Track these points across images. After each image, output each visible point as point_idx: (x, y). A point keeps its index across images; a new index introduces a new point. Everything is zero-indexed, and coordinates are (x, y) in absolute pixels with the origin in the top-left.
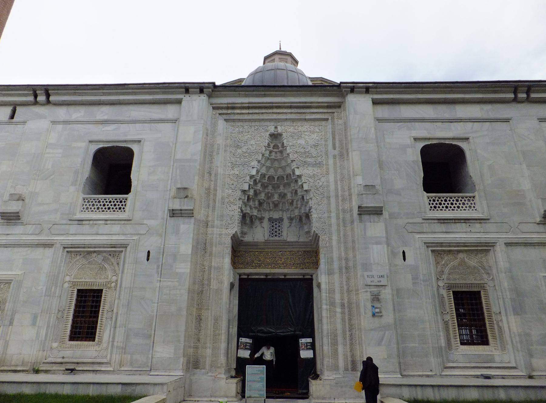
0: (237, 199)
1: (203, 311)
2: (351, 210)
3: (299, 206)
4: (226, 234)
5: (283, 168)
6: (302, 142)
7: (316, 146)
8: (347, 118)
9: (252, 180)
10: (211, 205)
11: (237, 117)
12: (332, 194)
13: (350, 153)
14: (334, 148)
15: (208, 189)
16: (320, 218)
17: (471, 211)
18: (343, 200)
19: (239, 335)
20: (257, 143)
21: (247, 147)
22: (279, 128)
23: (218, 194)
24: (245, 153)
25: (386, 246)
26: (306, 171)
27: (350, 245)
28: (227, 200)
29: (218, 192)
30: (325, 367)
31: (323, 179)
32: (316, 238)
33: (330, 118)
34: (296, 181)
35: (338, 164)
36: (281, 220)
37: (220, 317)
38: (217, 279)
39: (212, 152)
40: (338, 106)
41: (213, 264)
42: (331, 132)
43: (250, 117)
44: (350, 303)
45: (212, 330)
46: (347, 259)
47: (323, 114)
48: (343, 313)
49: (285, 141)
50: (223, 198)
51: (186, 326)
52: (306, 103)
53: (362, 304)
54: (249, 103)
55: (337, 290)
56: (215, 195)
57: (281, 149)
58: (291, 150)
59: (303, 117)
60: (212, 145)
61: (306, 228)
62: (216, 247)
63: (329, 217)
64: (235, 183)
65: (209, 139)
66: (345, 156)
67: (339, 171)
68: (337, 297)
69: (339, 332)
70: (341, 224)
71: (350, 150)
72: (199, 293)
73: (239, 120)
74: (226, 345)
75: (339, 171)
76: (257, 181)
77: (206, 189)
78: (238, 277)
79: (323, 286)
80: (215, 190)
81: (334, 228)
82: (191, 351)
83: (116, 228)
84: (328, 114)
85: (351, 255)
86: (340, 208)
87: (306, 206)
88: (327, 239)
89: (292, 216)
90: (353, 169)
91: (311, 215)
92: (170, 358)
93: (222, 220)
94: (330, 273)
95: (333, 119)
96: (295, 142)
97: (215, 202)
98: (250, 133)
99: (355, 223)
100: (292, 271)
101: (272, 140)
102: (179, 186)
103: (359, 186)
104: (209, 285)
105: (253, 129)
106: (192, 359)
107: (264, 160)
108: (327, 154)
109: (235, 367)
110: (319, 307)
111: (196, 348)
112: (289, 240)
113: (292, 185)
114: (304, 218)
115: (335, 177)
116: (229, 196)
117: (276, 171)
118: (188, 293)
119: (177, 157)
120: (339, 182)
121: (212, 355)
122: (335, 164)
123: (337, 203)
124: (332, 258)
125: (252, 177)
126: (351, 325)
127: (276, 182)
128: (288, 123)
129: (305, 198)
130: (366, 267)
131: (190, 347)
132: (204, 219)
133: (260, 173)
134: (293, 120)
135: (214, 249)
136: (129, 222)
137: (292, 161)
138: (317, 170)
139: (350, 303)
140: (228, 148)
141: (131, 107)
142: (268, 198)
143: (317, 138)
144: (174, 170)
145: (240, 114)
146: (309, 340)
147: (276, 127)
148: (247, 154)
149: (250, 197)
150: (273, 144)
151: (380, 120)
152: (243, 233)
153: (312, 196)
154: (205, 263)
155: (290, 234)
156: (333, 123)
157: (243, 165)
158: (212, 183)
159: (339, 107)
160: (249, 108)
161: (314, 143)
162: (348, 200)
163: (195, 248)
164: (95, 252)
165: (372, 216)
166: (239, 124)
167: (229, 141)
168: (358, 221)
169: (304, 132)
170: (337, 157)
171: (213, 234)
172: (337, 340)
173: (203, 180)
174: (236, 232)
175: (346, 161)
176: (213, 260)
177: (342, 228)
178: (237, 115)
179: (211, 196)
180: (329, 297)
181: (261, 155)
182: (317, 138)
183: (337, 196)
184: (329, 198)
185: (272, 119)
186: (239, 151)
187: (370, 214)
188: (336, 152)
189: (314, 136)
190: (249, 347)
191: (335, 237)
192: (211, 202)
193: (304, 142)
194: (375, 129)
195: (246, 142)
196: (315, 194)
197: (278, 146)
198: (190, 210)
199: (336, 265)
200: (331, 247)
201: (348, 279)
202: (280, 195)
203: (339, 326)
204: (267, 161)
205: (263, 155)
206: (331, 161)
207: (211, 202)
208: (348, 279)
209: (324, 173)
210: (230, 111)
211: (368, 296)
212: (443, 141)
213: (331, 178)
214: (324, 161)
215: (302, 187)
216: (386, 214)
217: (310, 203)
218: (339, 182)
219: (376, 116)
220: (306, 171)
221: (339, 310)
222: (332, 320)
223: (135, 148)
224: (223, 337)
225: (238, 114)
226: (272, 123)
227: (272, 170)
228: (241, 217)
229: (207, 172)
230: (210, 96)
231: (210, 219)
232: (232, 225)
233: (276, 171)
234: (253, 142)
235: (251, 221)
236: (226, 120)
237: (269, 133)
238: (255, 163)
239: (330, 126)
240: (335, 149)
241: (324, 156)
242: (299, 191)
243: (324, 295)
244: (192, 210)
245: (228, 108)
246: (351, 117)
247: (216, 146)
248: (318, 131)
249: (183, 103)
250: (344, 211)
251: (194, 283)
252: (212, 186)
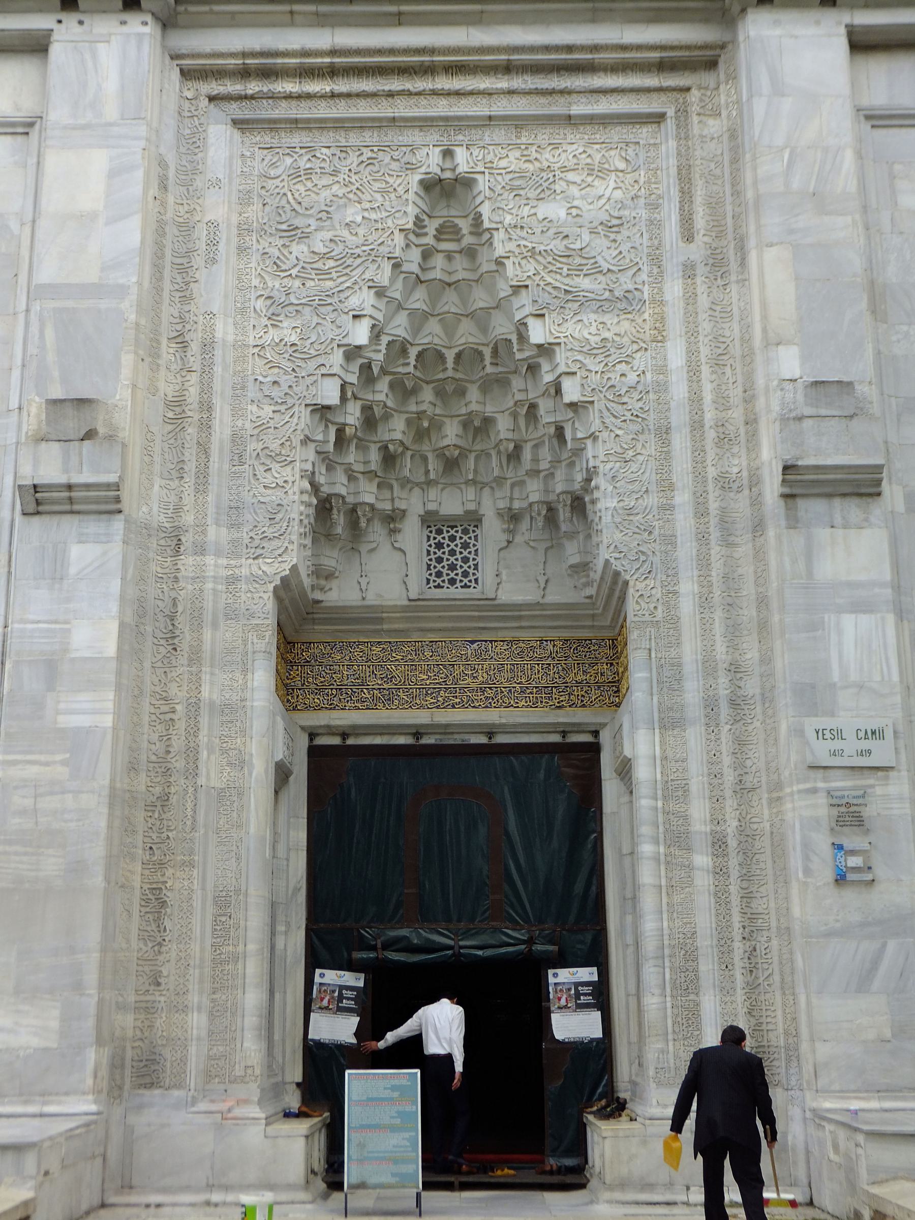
0: (296, 441)
1: (169, 872)
2: (755, 481)
3: (544, 465)
4: (255, 579)
5: (481, 319)
6: (555, 210)
7: (611, 227)
8: (740, 114)
9: (355, 367)
10: (191, 467)
11: (283, 110)
12: (679, 417)
13: (753, 257)
14: (689, 238)
15: (177, 403)
16: (630, 512)
18: (724, 440)
19: (314, 960)
20: (373, 216)
21: (328, 235)
22: (461, 156)
23: (216, 423)
24: (324, 256)
25: (891, 619)
26: (571, 328)
27: (749, 613)
28: (253, 446)
29: (217, 413)
30: (651, 1072)
31: (640, 361)
32: (615, 589)
33: (671, 112)
34: (533, 369)
35: (703, 301)
36: (472, 520)
37: (238, 891)
38: (224, 751)
39: (189, 254)
40: (707, 60)
41: (205, 693)
42: (673, 171)
43: (340, 110)
44: (747, 835)
45: (208, 942)
46: (735, 669)
47: (643, 97)
48: (720, 872)
49: (485, 210)
50: (237, 438)
51: (105, 928)
52: (570, 48)
53: (795, 839)
54: (333, 52)
55: (697, 782)
56: (206, 426)
57: (468, 240)
58: (511, 246)
59: (558, 107)
60: (186, 228)
61: (572, 553)
62: (215, 625)
63: (667, 508)
64: (285, 380)
65: (171, 199)
66: (734, 266)
67: (706, 326)
68: (699, 812)
69: (706, 942)
70: (715, 535)
71: (752, 243)
72: (153, 805)
73: (295, 124)
74: (265, 996)
75: (706, 326)
76: (376, 370)
77: (168, 405)
78: (303, 742)
79: (642, 772)
80: (207, 407)
81: (686, 550)
82: (127, 1021)
84: (663, 97)
85: (752, 655)
86: (712, 472)
87: (572, 465)
88: (658, 593)
89: (517, 505)
90: (765, 317)
91: (593, 502)
92: (46, 1050)
93: (235, 526)
94: (670, 721)
95: (683, 113)
96: (526, 211)
97: (206, 453)
98: (340, 178)
99: (771, 533)
100: (521, 719)
101: (433, 208)
102: (57, 393)
103: (789, 386)
104: (192, 772)
105: (353, 159)
106: (129, 1054)
107: (399, 285)
108: (656, 260)
109: (299, 1078)
110: (626, 850)
111: (147, 1009)
112: (507, 595)
113: (517, 383)
114: (563, 514)
115: (692, 353)
116: (262, 428)
117: (449, 330)
118: (111, 806)
119: (46, 274)
120: (705, 370)
121: (211, 1033)
122: (690, 298)
123: (699, 451)
124: (678, 665)
125: (352, 353)
126: (751, 920)
127: (450, 373)
128: (499, 135)
129: (568, 435)
130: (813, 696)
131: (121, 1007)
132: (160, 518)
133: (385, 339)
134: (518, 123)
135: (207, 635)
137: (517, 289)
138: (617, 326)
139: (747, 835)
140: (251, 240)
142: (421, 435)
143: (618, 194)
144: (34, 329)
145: (299, 97)
146: (588, 974)
147: (448, 153)
148: (331, 263)
149: (349, 431)
150: (436, 223)
151: (877, 119)
152: (323, 575)
153: (596, 425)
154: (173, 689)
155: (508, 575)
156: (683, 135)
157: (319, 304)
158: (194, 378)
159: (712, 64)
160: (333, 72)
161: (604, 217)
162: (742, 438)
163: (131, 635)
165: (837, 502)
166: (297, 139)
167: (254, 212)
168: (783, 523)
169: (564, 169)
170: (701, 270)
171: (199, 578)
172: (696, 971)
173: (155, 368)
174: (294, 568)
175: (734, 288)
176: (206, 677)
177: (716, 550)
178: (284, 104)
179: (190, 430)
180: (666, 813)
181: (387, 267)
182: (618, 194)
183: (697, 426)
184: (664, 433)
185: (432, 119)
186: (299, 250)
187: (830, 496)
188: (696, 252)
189: (606, 187)
190: (351, 1004)
191: (688, 587)
192: (191, 454)
193: (562, 213)
194: (859, 155)
195: (325, 215)
196: (609, 420)
197: (456, 230)
198: (108, 486)
199: (692, 693)
200: (674, 622)
201: (741, 743)
202: (465, 425)
203: (704, 921)
204: (412, 291)
205: (396, 266)
206: (674, 289)
207: (191, 454)
208: (741, 743)
209: (647, 337)
210: (253, 87)
211: (820, 808)
213: (676, 355)
214: (646, 289)
215: (558, 391)
216: (893, 495)
217: (590, 452)
218: (705, 370)
219: (865, 102)
220: (571, 328)
221: (702, 860)
222: (677, 899)
224: (253, 968)
225: (289, 97)
226: (433, 136)
227: (433, 326)
228: (311, 511)
229: (173, 332)
232: (276, 543)
233: (449, 330)
234: (353, 213)
235: (353, 523)
236: (239, 124)
237: (418, 177)
238: (364, 299)
239: (672, 144)
240: (689, 238)
241: (645, 269)
242: (544, 406)
243: (644, 803)
244: (117, 487)
245: (245, 73)
246: (759, 107)
247: (201, 233)
248: (622, 165)
249: (56, 49)
250: (725, 483)
251: (132, 768)
252: (193, 394)
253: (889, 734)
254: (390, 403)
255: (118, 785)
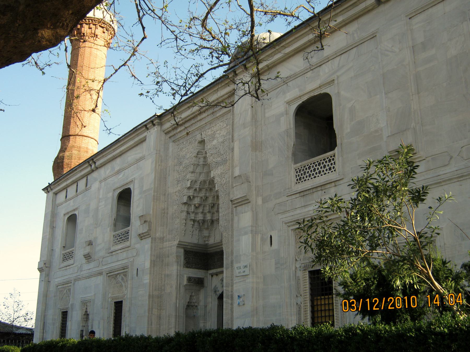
17: (330, 173)
80: (168, 209)
83: (124, 255)
118: (149, 298)
134: (210, 122)
136: (129, 249)
141: (129, 154)
164: (118, 274)
204: (203, 168)
212: (312, 94)
223: (131, 187)
230: (161, 124)
231: (165, 235)
238: (189, 176)
253: (248, 266)
254: (207, 195)
255: (151, 294)
